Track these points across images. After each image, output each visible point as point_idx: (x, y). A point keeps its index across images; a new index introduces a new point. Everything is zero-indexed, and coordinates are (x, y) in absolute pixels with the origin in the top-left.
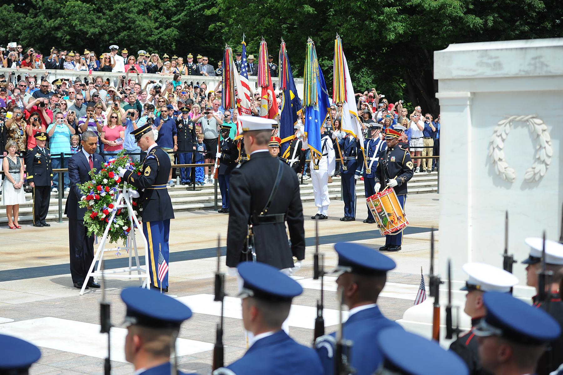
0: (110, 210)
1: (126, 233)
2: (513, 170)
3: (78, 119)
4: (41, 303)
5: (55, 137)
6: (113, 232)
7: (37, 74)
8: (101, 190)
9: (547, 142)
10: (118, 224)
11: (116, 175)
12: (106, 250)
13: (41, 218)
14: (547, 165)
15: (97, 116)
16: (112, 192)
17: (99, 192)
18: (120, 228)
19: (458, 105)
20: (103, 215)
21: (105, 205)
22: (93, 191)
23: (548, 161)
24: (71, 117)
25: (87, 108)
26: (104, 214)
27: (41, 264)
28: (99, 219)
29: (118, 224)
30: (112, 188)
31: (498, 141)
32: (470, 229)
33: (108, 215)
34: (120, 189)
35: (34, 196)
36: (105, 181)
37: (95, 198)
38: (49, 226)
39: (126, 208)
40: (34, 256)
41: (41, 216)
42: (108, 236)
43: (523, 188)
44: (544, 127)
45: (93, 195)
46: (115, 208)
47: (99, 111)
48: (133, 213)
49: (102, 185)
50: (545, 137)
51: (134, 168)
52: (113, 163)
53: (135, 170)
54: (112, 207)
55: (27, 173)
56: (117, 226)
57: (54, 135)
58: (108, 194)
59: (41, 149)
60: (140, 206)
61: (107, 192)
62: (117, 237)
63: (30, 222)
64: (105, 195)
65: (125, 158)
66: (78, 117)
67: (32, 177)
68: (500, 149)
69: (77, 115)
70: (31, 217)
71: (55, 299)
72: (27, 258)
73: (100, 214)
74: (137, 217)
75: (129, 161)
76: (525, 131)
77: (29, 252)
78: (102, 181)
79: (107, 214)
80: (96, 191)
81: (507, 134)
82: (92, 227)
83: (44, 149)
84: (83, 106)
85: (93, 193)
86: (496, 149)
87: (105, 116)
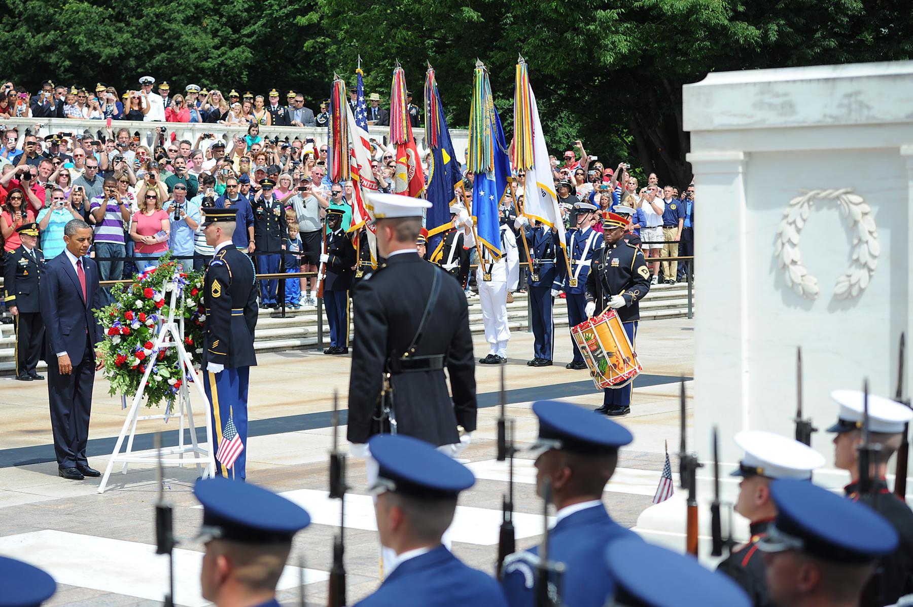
0: (147, 352)
1: (174, 389)
2: (815, 280)
3: (89, 200)
4: (35, 507)
5: (51, 229)
6: (152, 388)
7: (18, 125)
8: (132, 319)
9: (871, 233)
10: (161, 375)
11: (157, 292)
12: (141, 418)
13: (29, 366)
14: (870, 270)
15: (121, 196)
16: (149, 322)
17: (128, 322)
18: (164, 382)
19: (724, 173)
20: (135, 361)
21: (139, 344)
22: (119, 320)
23: (873, 264)
24: (77, 197)
25: (105, 183)
26: (137, 359)
27: (32, 442)
28: (129, 367)
29: (161, 375)
30: (151, 315)
31: (790, 232)
32: (746, 378)
33: (145, 361)
34: (162, 317)
35: (17, 329)
36: (139, 304)
37: (122, 333)
39: (174, 348)
40: (19, 429)
41: (29, 363)
42: (144, 394)
43: (831, 309)
44: (866, 208)
45: (119, 326)
46: (156, 349)
47: (123, 186)
48: (185, 357)
49: (133, 310)
50: (867, 225)
51: (187, 282)
53: (188, 285)
54: (150, 346)
55: (6, 292)
56: (159, 378)
57: (48, 228)
58: (143, 325)
59: (29, 251)
60: (197, 346)
61: (142, 322)
63: (10, 373)
64: (139, 327)
65: (171, 264)
66: (89, 196)
67: (13, 297)
68: (794, 245)
69: (88, 193)
70: (13, 365)
71: (57, 500)
72: (8, 432)
74: (193, 362)
76: (834, 214)
77: (10, 423)
78: (134, 303)
79: (143, 358)
80: (123, 320)
81: (804, 220)
82: (117, 380)
83: (33, 250)
84: (97, 179)
85: (118, 324)
86: (787, 246)
87: (135, 196)
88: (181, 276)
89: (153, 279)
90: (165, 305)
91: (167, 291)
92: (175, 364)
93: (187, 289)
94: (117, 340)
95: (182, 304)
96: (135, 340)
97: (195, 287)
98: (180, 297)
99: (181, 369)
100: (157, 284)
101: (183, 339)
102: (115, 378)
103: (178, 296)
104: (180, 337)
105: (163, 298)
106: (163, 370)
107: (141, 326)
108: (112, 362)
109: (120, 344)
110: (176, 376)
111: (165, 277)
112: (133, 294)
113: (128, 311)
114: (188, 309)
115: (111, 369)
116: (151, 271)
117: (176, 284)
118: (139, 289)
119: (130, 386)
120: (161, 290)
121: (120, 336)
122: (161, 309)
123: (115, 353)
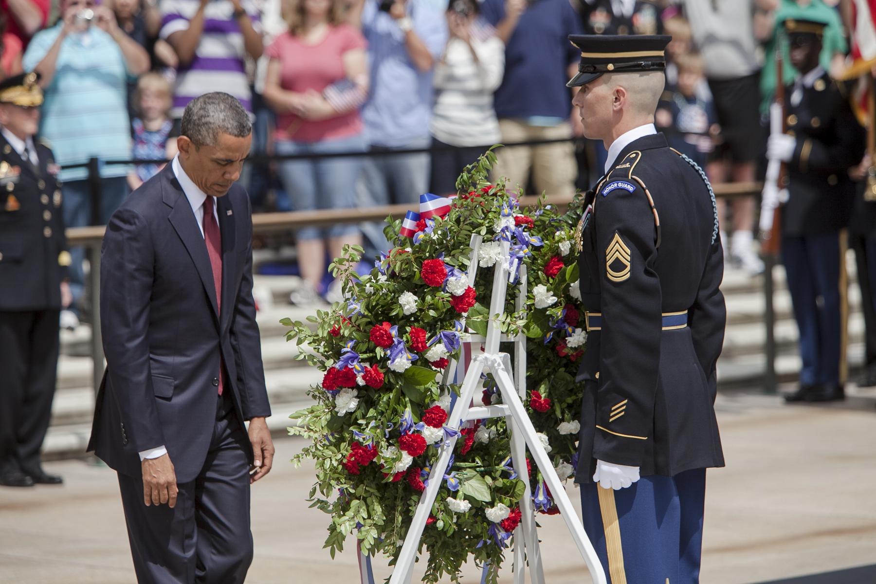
0: (430, 433)
1: (501, 534)
6: (444, 532)
8: (388, 344)
10: (466, 497)
13: (23, 451)
16: (437, 351)
18: (475, 515)
20: (398, 459)
21: (408, 414)
22: (353, 348)
26: (405, 453)
29: (466, 497)
30: (440, 333)
36: (409, 302)
37: (360, 381)
38: (54, 481)
41: (23, 441)
42: (420, 550)
45: (356, 366)
46: (453, 424)
49: (393, 321)
52: (442, 217)
53: (536, 249)
54: (438, 418)
56: (463, 506)
60: (563, 413)
61: (417, 349)
62: (455, 555)
64: (408, 365)
65: (491, 192)
73: (387, 453)
75: (511, 208)
78: (395, 301)
80: (364, 347)
82: (350, 513)
85: (353, 359)
88: (518, 223)
89: (444, 234)
90: (477, 306)
91: (482, 264)
92: (502, 466)
93: (534, 259)
94: (347, 402)
95: (522, 301)
96: (398, 401)
97: (557, 253)
98: (517, 282)
99: (518, 477)
100: (455, 246)
101: (524, 398)
102: (343, 506)
103: (512, 280)
104: (517, 390)
105: (472, 286)
106: (473, 482)
107: (413, 363)
108: (335, 464)
109: (359, 414)
110: (507, 500)
111: (475, 226)
112: (393, 276)
113: (381, 322)
114: (538, 315)
115: (333, 482)
116: (437, 210)
117: (507, 245)
118: (408, 262)
119: (386, 527)
120: (466, 262)
121: (355, 392)
122: (465, 314)
123: (342, 439)
